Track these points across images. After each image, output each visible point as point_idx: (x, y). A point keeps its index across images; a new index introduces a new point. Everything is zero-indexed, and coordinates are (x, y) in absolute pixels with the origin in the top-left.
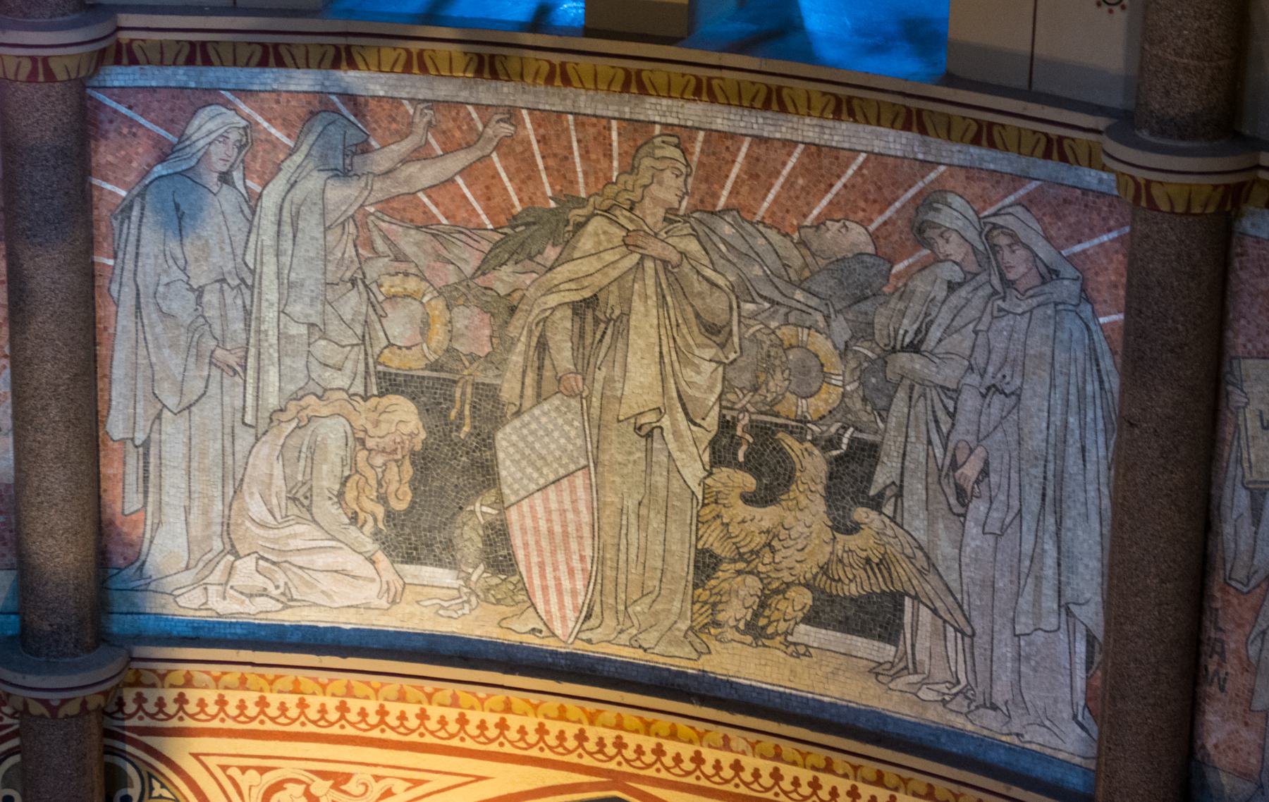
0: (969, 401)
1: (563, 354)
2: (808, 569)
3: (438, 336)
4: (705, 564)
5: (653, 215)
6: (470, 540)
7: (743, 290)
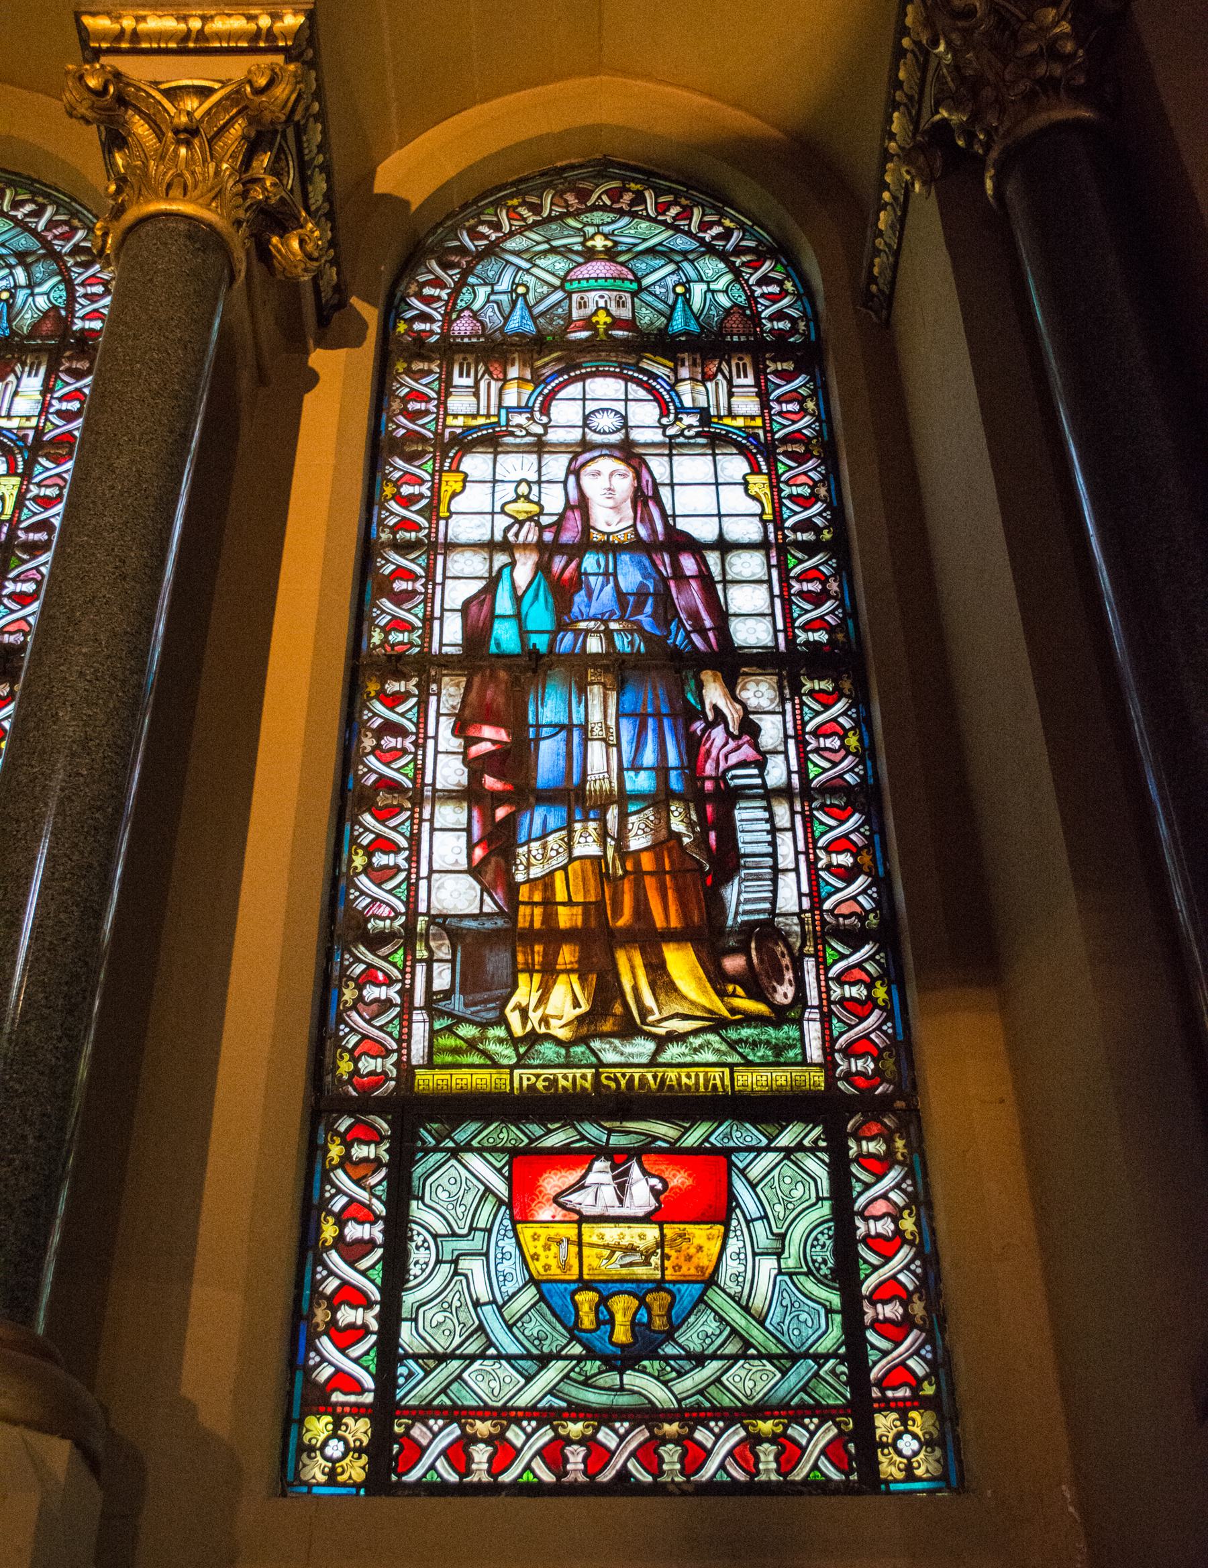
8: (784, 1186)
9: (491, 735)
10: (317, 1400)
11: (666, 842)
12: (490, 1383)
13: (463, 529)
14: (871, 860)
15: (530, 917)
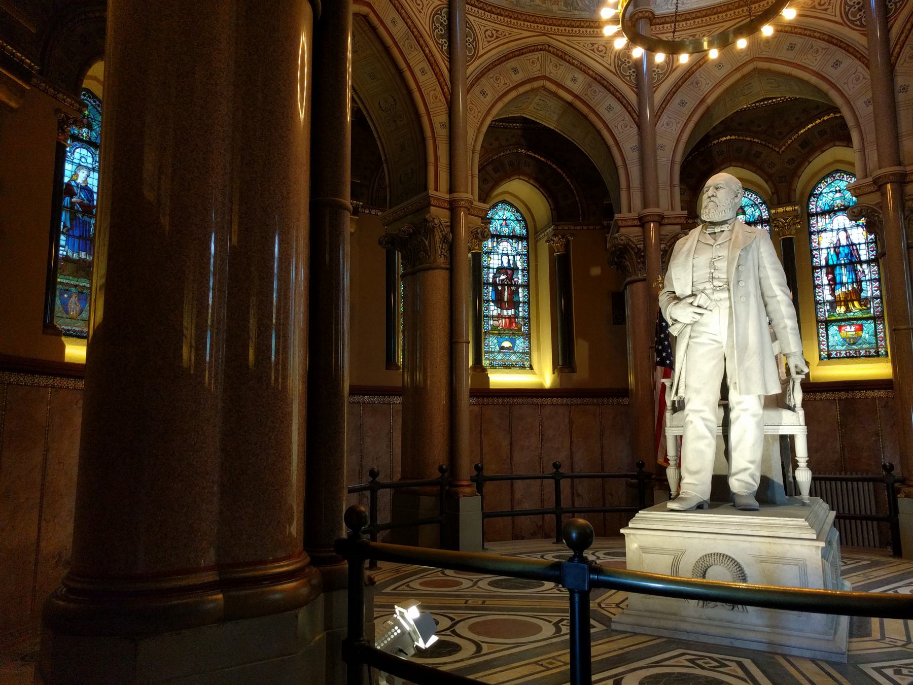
8: (869, 326)
9: (830, 276)
11: (853, 288)
13: (822, 246)
14: (879, 288)
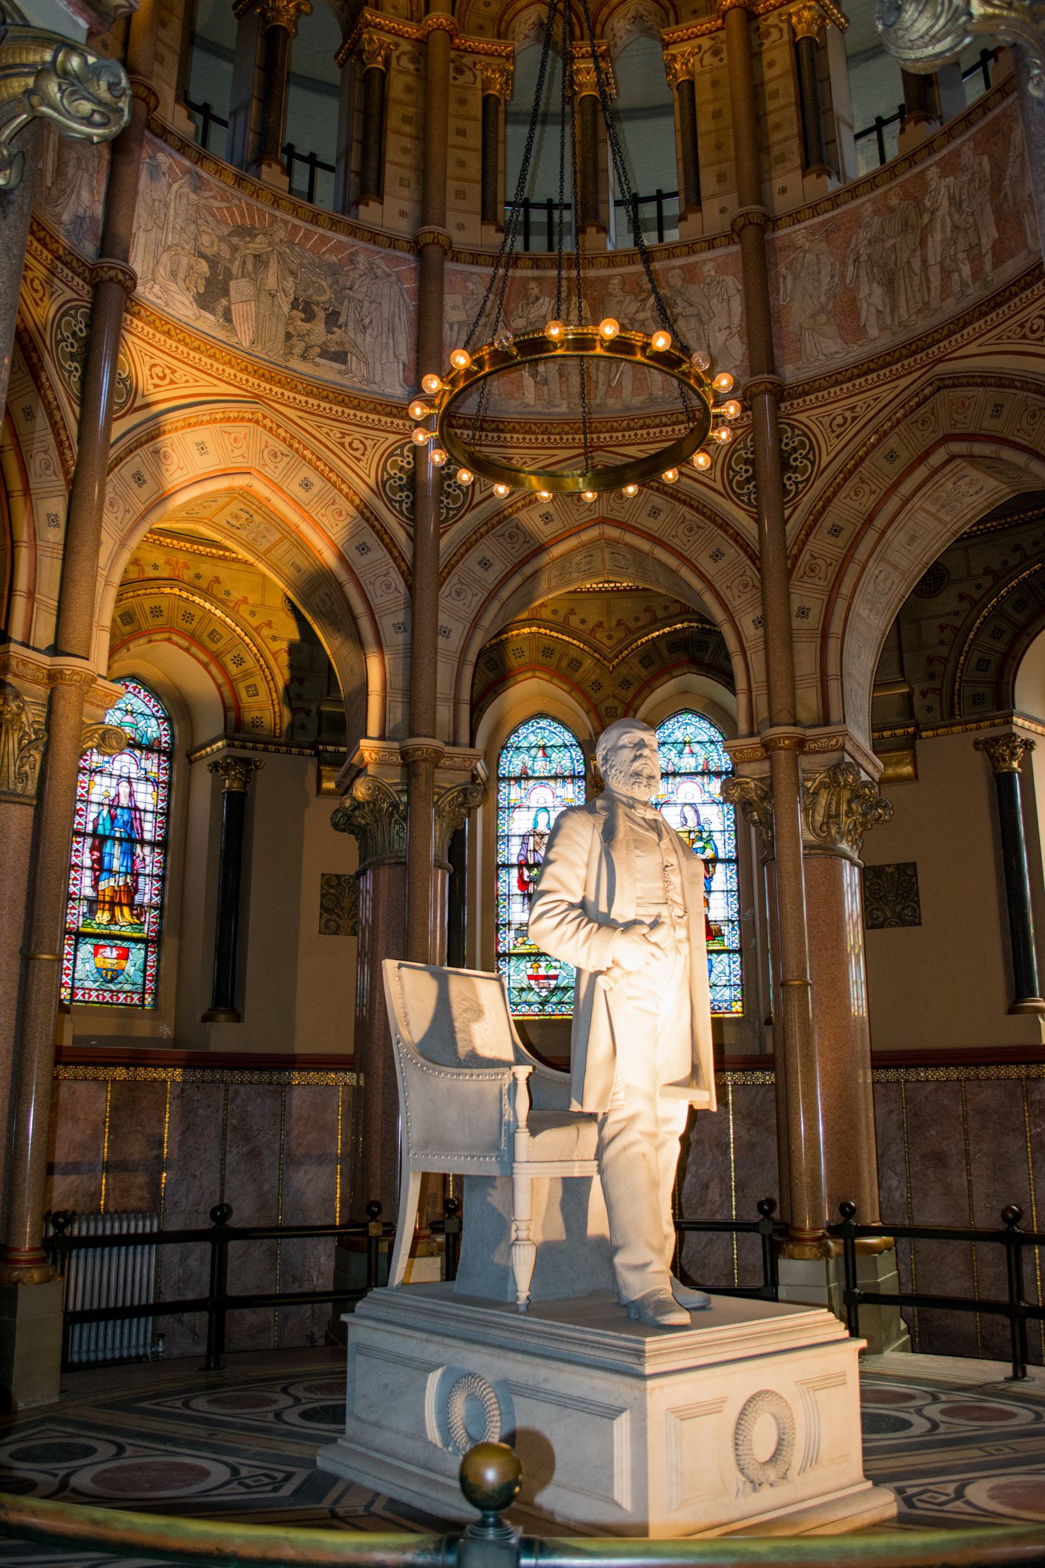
0: (366, 304)
1: (250, 267)
2: (320, 342)
3: (215, 248)
4: (288, 336)
5: (277, 240)
6: (220, 310)
7: (302, 265)
8: (137, 954)
10: (62, 985)
11: (126, 884)
12: (88, 984)
14: (161, 892)
15: (101, 898)
